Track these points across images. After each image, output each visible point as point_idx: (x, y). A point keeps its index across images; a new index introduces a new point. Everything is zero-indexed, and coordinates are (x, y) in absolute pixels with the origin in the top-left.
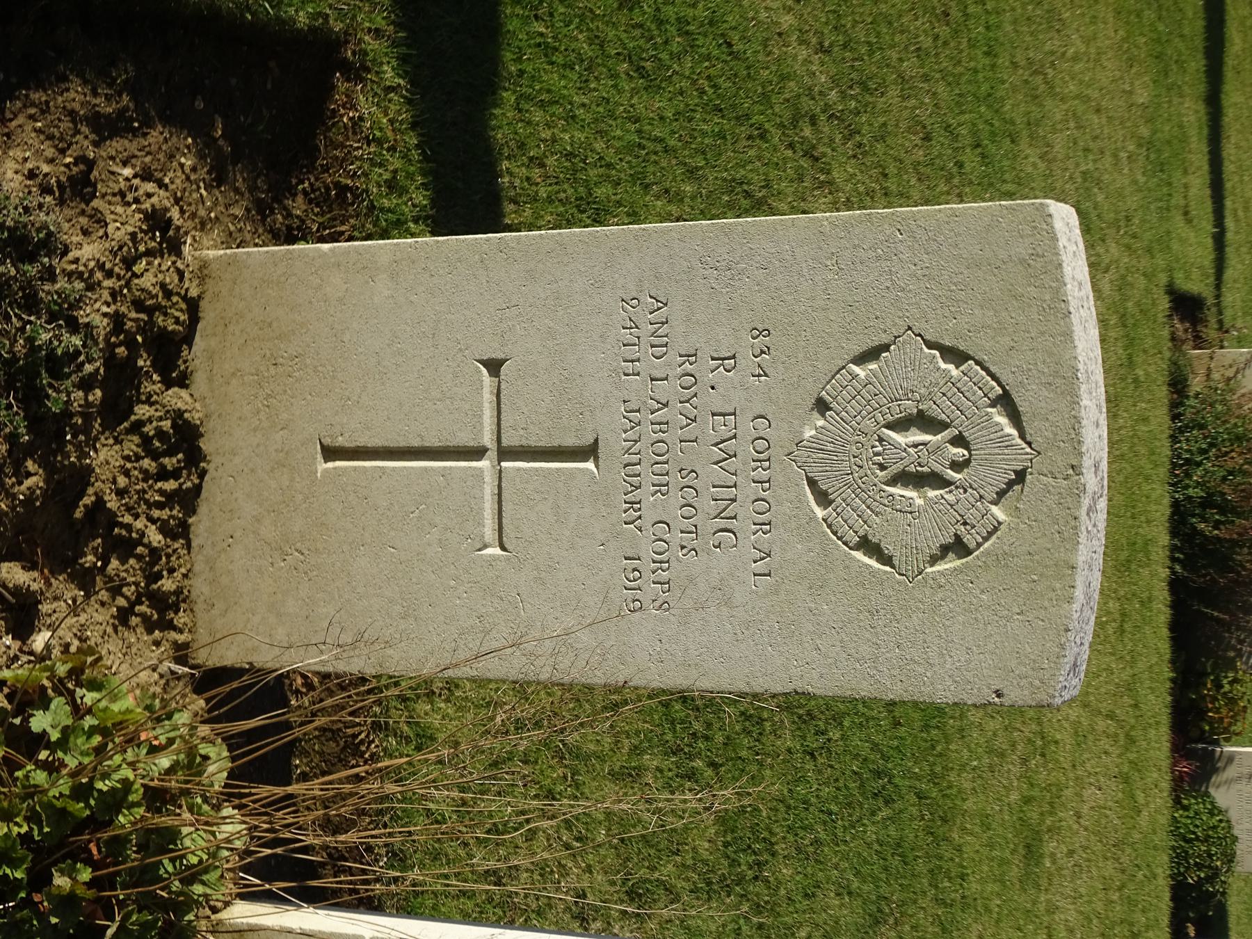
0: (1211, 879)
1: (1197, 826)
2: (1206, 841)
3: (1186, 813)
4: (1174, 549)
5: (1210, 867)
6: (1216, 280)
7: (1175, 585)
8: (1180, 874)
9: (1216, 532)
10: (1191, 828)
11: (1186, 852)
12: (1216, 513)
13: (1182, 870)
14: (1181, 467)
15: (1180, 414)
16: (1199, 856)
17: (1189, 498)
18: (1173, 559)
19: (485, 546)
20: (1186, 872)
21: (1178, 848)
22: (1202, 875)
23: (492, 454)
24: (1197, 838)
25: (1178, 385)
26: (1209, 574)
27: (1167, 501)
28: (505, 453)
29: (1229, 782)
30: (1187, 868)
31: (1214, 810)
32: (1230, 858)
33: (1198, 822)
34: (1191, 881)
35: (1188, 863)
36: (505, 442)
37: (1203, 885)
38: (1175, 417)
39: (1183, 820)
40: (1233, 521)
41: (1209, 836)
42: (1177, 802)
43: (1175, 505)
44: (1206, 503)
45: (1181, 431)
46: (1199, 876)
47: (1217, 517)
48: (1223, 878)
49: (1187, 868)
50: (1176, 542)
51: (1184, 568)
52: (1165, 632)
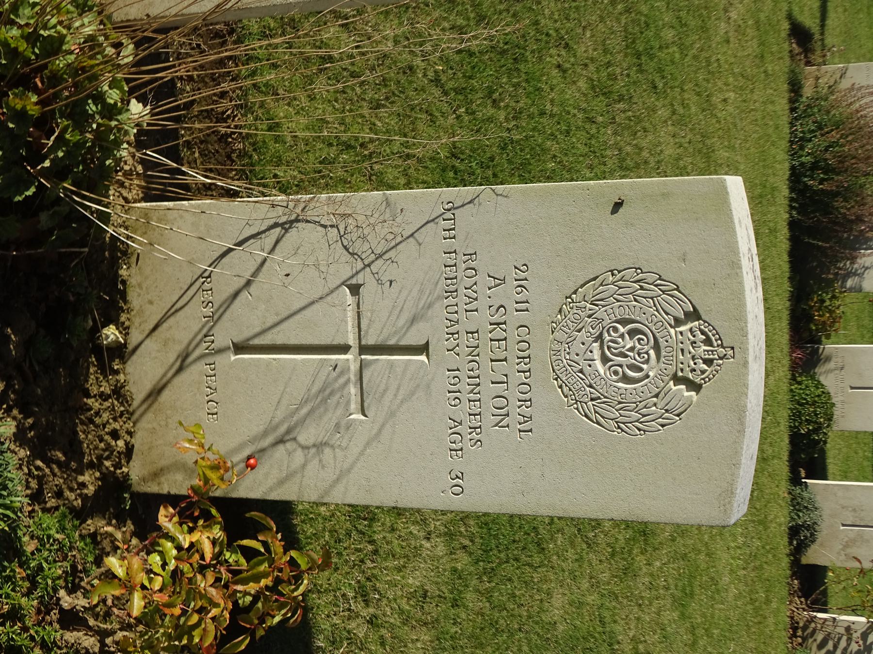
0: (816, 431)
1: (807, 395)
2: (814, 405)
3: (800, 387)
4: (792, 200)
5: (816, 422)
6: (821, 22)
7: (792, 225)
8: (795, 427)
9: (821, 186)
10: (803, 396)
11: (800, 412)
12: (821, 173)
13: (797, 424)
14: (797, 143)
15: (796, 108)
16: (809, 415)
17: (802, 164)
18: (792, 208)
19: (350, 414)
20: (799, 425)
21: (794, 409)
22: (811, 428)
23: (355, 350)
24: (807, 403)
25: (795, 87)
26: (816, 216)
27: (787, 165)
28: (364, 349)
29: (831, 371)
30: (800, 423)
31: (819, 385)
32: (830, 418)
33: (808, 392)
34: (803, 432)
35: (801, 419)
36: (363, 343)
37: (811, 435)
38: (793, 110)
39: (797, 391)
40: (833, 178)
41: (816, 402)
42: (794, 378)
43: (793, 168)
44: (814, 166)
45: (796, 119)
46: (808, 428)
47: (822, 176)
48: (824, 431)
49: (800, 423)
50: (793, 195)
51: (798, 213)
52: (786, 257)
